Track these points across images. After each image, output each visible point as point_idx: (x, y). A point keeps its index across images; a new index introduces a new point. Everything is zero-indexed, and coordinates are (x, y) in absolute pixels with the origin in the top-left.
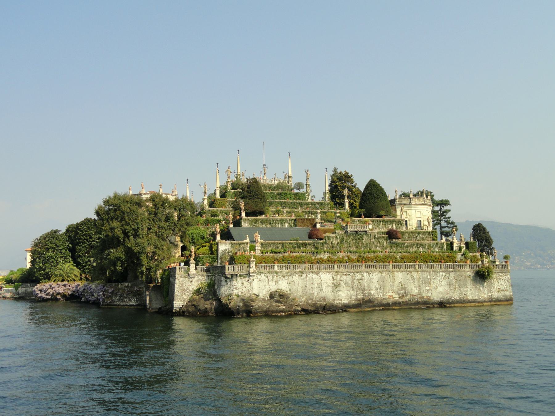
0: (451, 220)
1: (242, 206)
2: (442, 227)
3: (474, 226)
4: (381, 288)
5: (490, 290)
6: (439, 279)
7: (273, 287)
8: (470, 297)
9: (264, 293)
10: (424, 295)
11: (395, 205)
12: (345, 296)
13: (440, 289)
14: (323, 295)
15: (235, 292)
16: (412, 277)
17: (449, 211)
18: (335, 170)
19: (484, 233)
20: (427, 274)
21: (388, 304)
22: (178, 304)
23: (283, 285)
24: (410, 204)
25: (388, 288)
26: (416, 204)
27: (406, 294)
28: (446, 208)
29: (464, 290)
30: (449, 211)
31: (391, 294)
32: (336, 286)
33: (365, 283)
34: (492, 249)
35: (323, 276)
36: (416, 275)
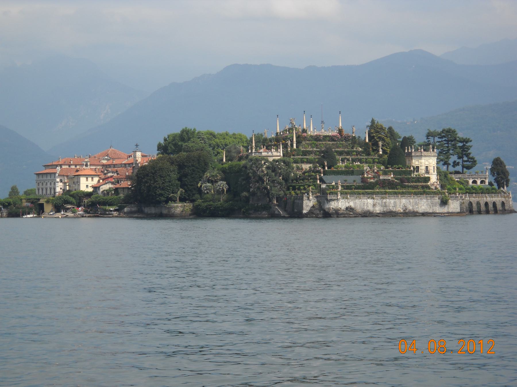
0: (471, 156)
1: (326, 164)
2: (463, 161)
3: (494, 160)
4: (395, 206)
5: (448, 208)
6: (423, 202)
7: (347, 205)
8: (438, 212)
9: (343, 207)
10: (415, 210)
11: (412, 156)
12: (378, 209)
13: (423, 207)
14: (368, 209)
15: (331, 207)
16: (410, 202)
17: (471, 147)
18: (373, 121)
19: (501, 167)
20: (417, 200)
21: (398, 213)
22: (305, 212)
23: (352, 204)
24: (421, 156)
25: (398, 206)
26: (425, 156)
27: (406, 209)
28: (469, 144)
29: (434, 208)
30: (471, 147)
31: (399, 209)
32: (374, 205)
33: (387, 204)
34: (508, 181)
35: (369, 200)
36: (411, 201)
